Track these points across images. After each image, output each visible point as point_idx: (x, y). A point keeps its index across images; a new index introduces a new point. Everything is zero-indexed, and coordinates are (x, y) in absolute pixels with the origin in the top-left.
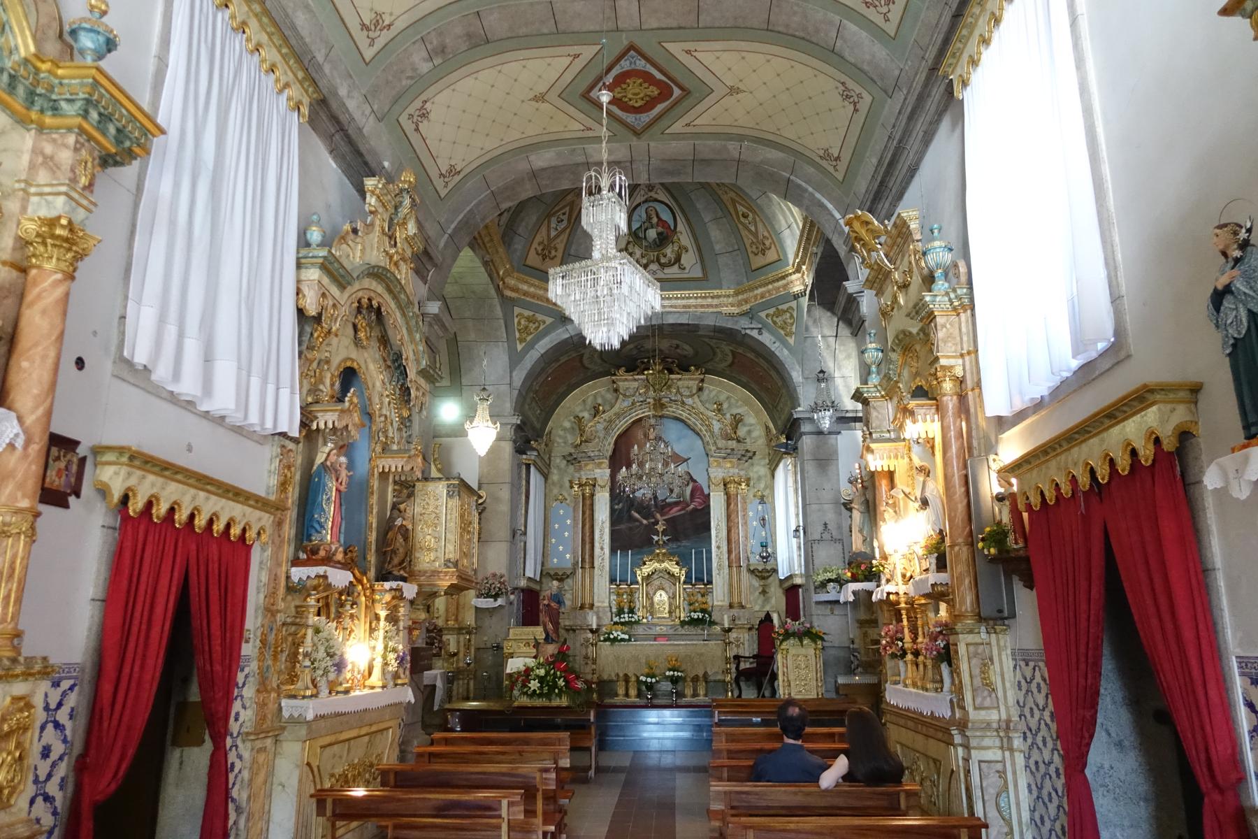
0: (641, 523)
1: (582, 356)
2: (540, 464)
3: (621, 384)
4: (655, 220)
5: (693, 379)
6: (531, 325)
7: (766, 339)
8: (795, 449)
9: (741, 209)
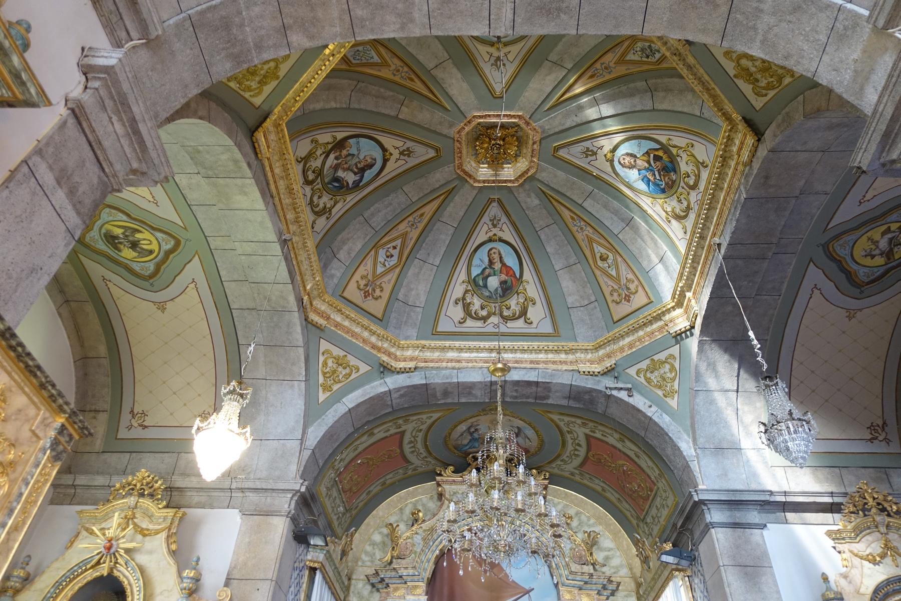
1: (403, 433)
2: (331, 574)
3: (447, 487)
4: (497, 266)
6: (340, 369)
7: (638, 401)
8: (693, 559)
9: (599, 250)
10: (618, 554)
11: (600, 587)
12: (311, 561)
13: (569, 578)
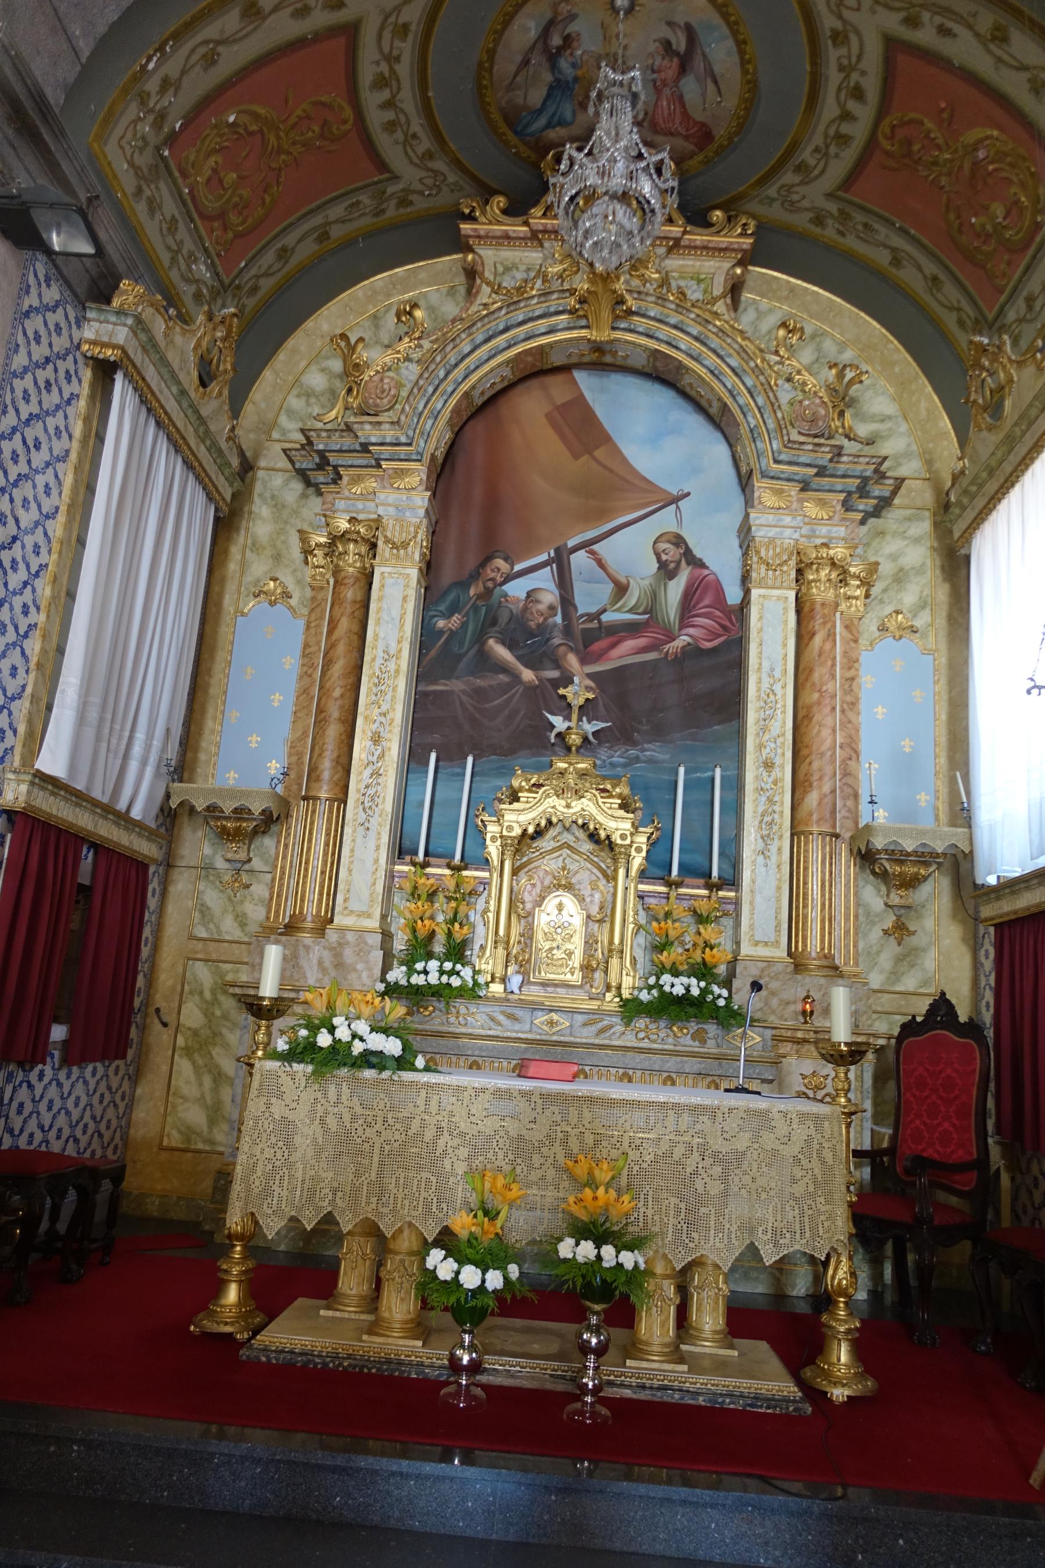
0: (516, 678)
5: (722, 251)
10: (904, 427)
11: (853, 483)
12: (94, 343)
13: (783, 457)
